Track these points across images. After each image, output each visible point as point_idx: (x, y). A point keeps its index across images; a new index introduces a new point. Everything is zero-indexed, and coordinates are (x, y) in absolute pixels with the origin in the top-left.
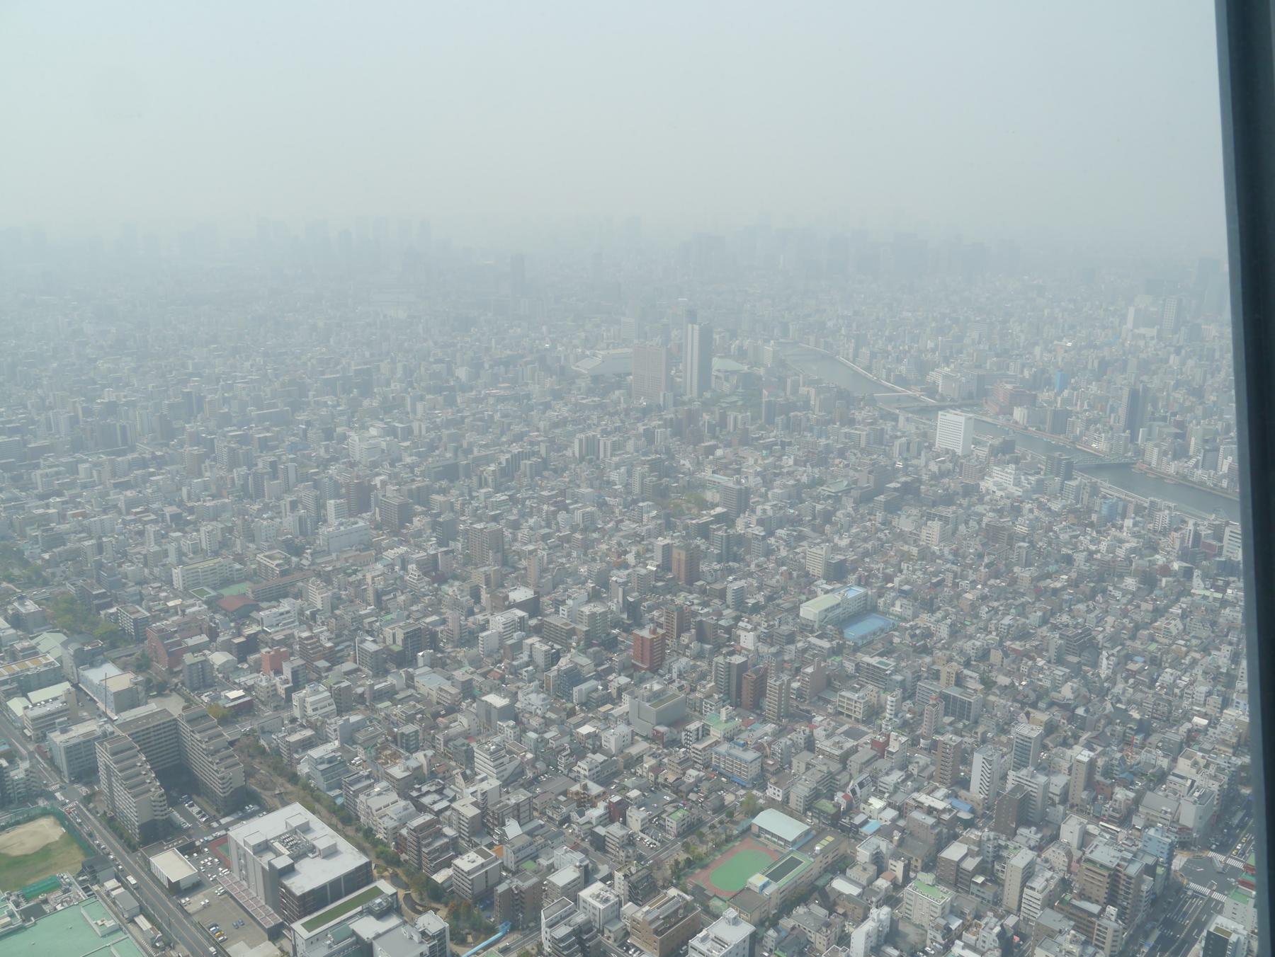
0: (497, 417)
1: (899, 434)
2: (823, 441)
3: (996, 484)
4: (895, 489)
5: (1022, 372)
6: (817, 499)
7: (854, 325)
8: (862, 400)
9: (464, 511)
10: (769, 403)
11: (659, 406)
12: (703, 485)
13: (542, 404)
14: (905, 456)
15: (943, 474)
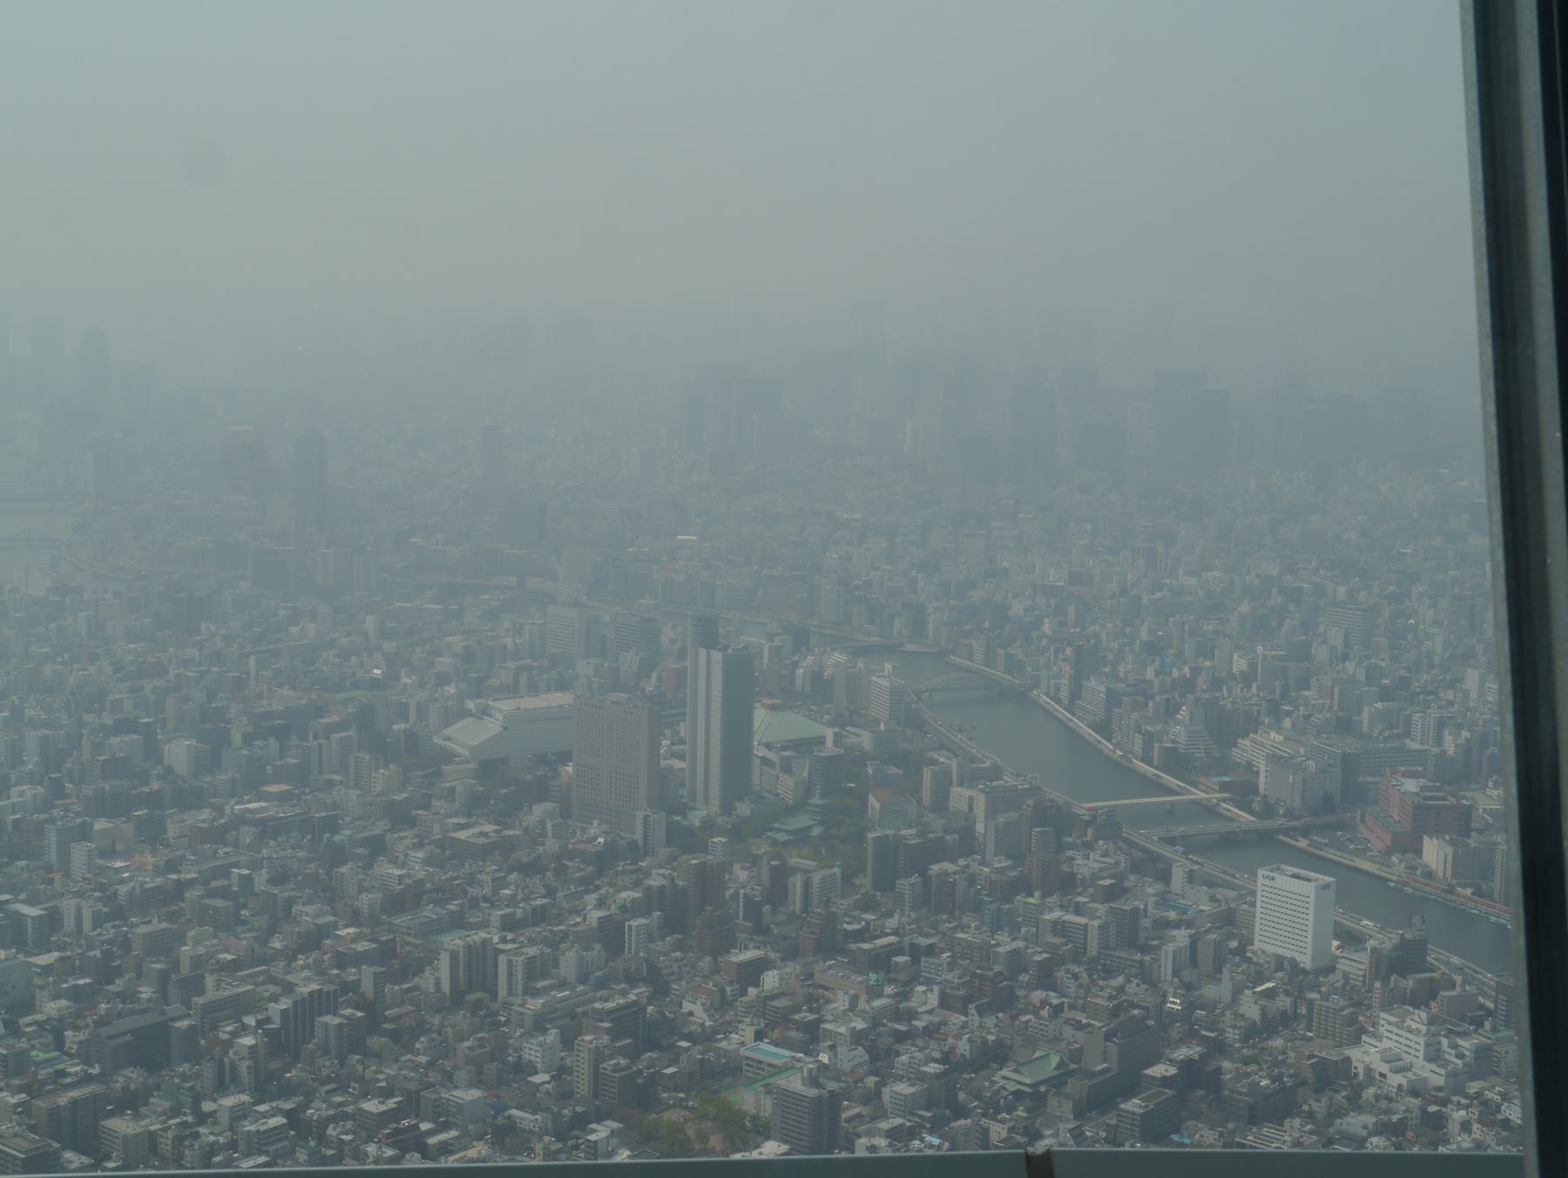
0: (261, 879)
1: (1172, 915)
2: (1006, 944)
3: (1389, 1059)
4: (1165, 1081)
5: (1439, 741)
6: (993, 1107)
7: (1071, 611)
8: (1088, 824)
9: (181, 1156)
10: (882, 841)
11: (633, 845)
12: (736, 1069)
13: (364, 842)
14: (1187, 975)
15: (1271, 1025)
